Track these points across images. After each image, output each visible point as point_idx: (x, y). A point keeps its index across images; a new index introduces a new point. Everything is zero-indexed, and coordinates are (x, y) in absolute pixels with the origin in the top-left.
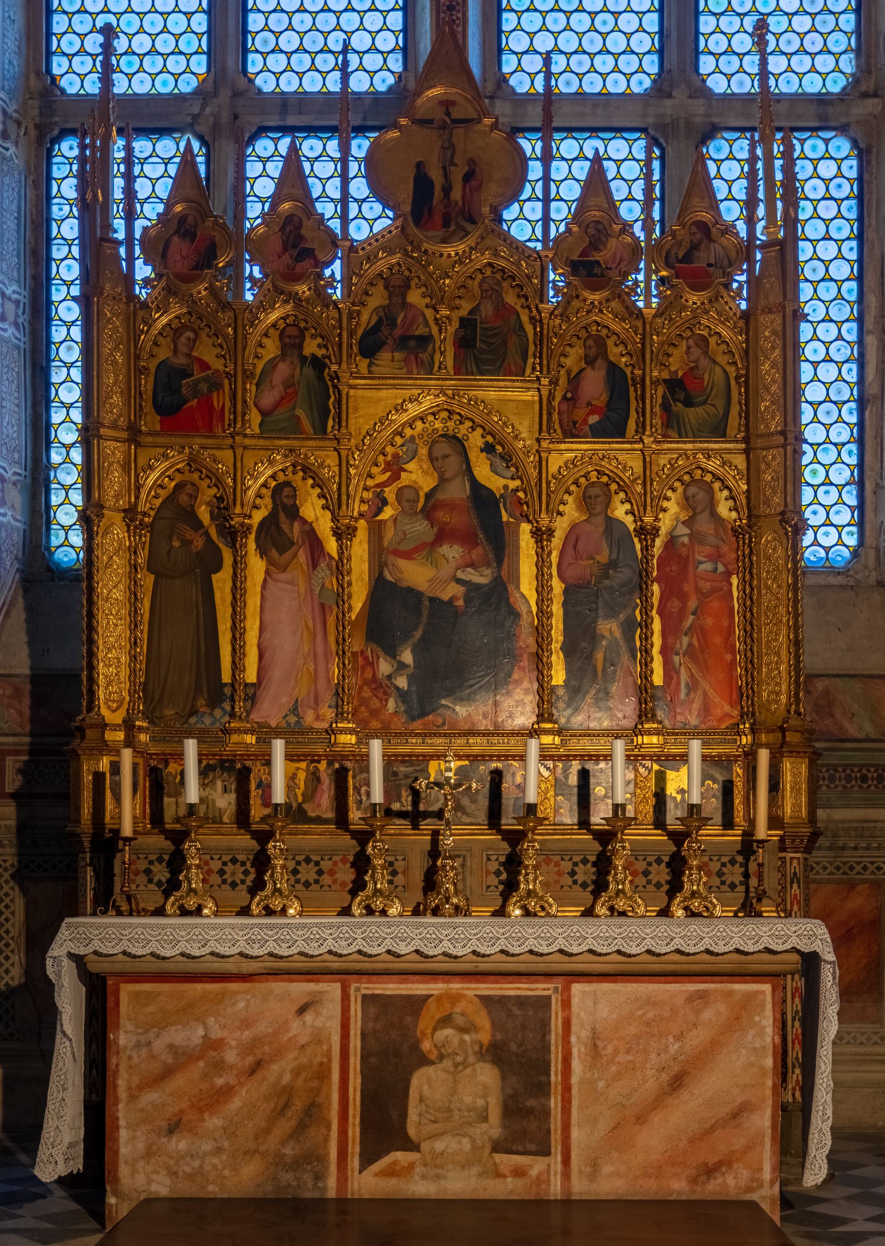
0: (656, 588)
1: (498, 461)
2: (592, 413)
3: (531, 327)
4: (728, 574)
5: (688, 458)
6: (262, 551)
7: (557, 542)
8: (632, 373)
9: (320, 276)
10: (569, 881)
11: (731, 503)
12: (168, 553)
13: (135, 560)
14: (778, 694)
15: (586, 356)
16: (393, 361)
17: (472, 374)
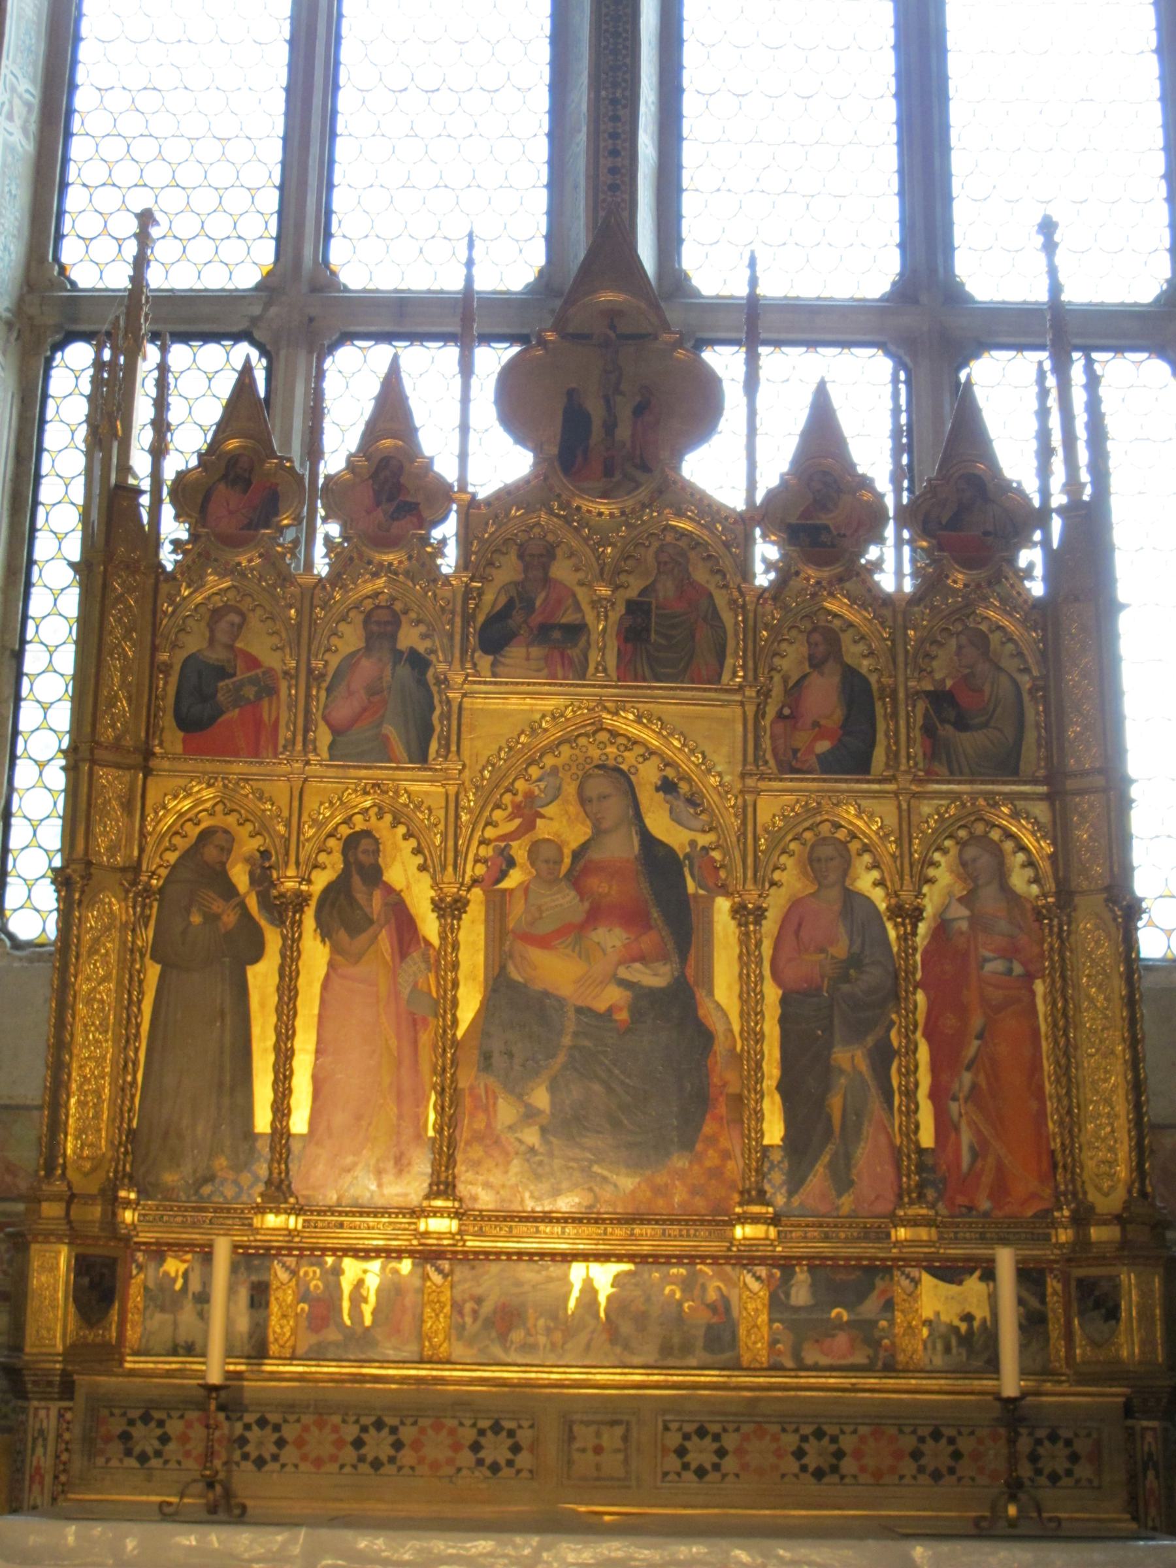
0: (920, 997)
1: (680, 805)
2: (821, 736)
3: (731, 614)
4: (1029, 977)
5: (963, 805)
6: (325, 931)
7: (770, 926)
8: (879, 681)
9: (425, 540)
10: (794, 1466)
11: (1029, 873)
12: (184, 932)
13: (134, 942)
14: (1111, 1164)
15: (811, 658)
16: (528, 659)
17: (644, 680)
